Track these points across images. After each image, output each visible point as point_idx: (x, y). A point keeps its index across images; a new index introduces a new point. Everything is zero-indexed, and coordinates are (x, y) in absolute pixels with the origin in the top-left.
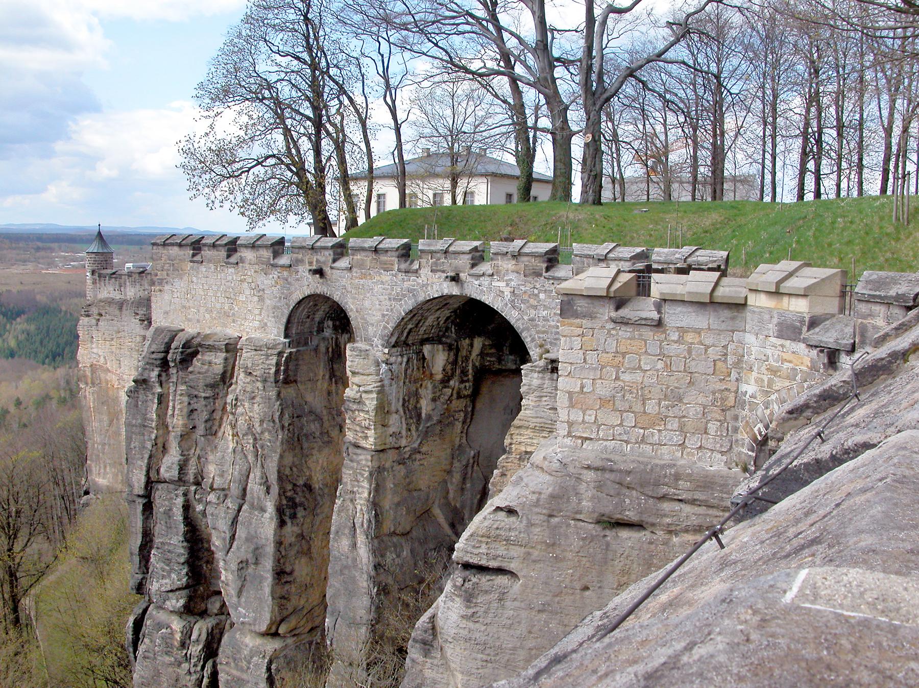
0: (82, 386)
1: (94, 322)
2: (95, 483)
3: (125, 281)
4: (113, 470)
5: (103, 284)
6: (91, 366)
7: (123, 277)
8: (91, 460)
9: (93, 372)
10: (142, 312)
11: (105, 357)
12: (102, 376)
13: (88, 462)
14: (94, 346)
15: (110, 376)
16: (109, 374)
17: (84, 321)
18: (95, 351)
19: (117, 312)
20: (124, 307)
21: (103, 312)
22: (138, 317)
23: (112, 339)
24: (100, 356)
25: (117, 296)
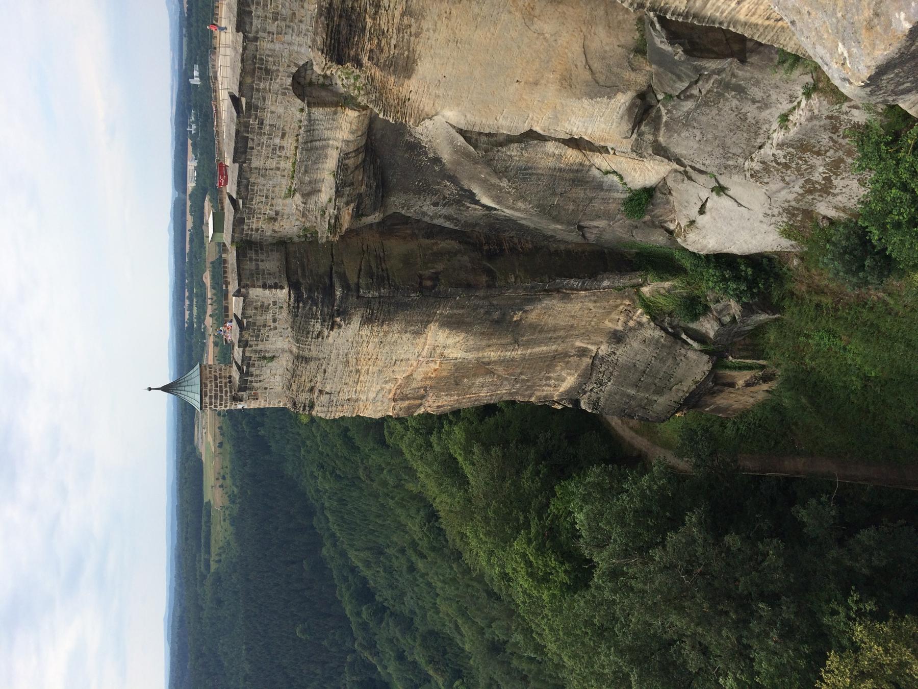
0: (421, 411)
1: (324, 398)
2: (567, 392)
3: (256, 351)
4: (559, 368)
5: (258, 385)
6: (394, 400)
7: (247, 354)
8: (531, 396)
9: (405, 398)
10: (318, 326)
11: (386, 382)
12: (414, 385)
13: (533, 399)
14: (363, 397)
15: (418, 376)
16: (415, 376)
17: (318, 412)
18: (372, 395)
19: (313, 365)
20: (306, 354)
21: (308, 385)
22: (326, 333)
23: (358, 371)
24: (382, 389)
25: (284, 362)
